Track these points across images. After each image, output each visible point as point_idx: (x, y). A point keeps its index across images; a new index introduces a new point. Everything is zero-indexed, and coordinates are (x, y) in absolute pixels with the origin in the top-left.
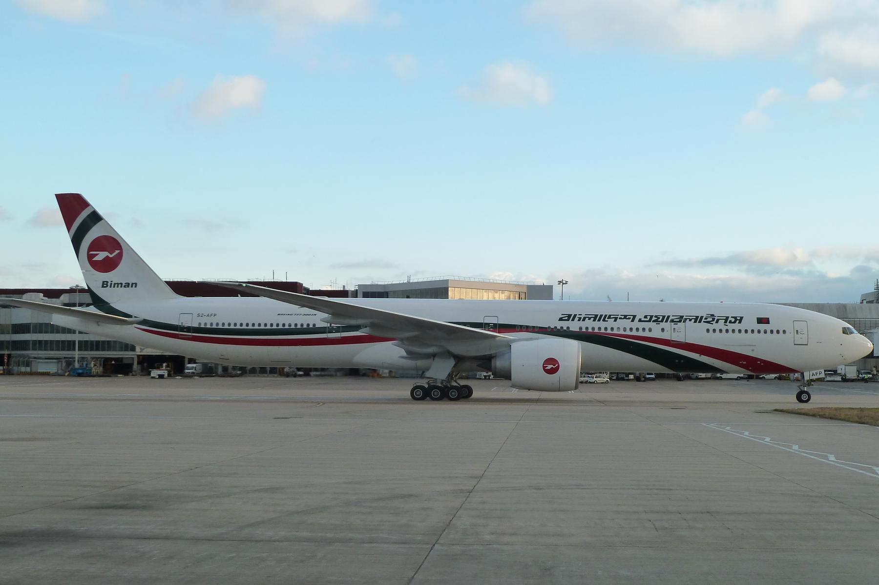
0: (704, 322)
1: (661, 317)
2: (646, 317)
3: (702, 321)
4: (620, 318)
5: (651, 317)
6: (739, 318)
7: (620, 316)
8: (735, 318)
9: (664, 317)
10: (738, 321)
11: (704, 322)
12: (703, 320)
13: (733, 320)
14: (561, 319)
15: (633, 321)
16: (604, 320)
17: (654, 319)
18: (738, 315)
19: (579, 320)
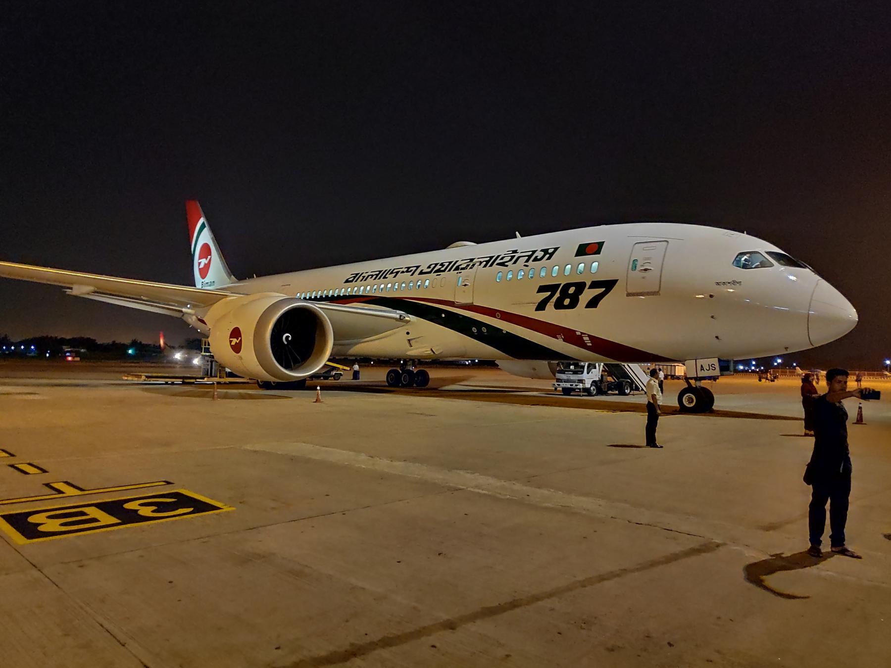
0: (498, 264)
1: (446, 264)
2: (429, 267)
3: (495, 263)
4: (403, 272)
5: (436, 265)
6: (550, 251)
7: (401, 270)
8: (546, 251)
9: (450, 263)
10: (548, 256)
11: (498, 264)
12: (498, 261)
13: (540, 254)
14: (347, 281)
15: (412, 275)
16: (385, 277)
17: (438, 267)
18: (550, 247)
19: (361, 281)
